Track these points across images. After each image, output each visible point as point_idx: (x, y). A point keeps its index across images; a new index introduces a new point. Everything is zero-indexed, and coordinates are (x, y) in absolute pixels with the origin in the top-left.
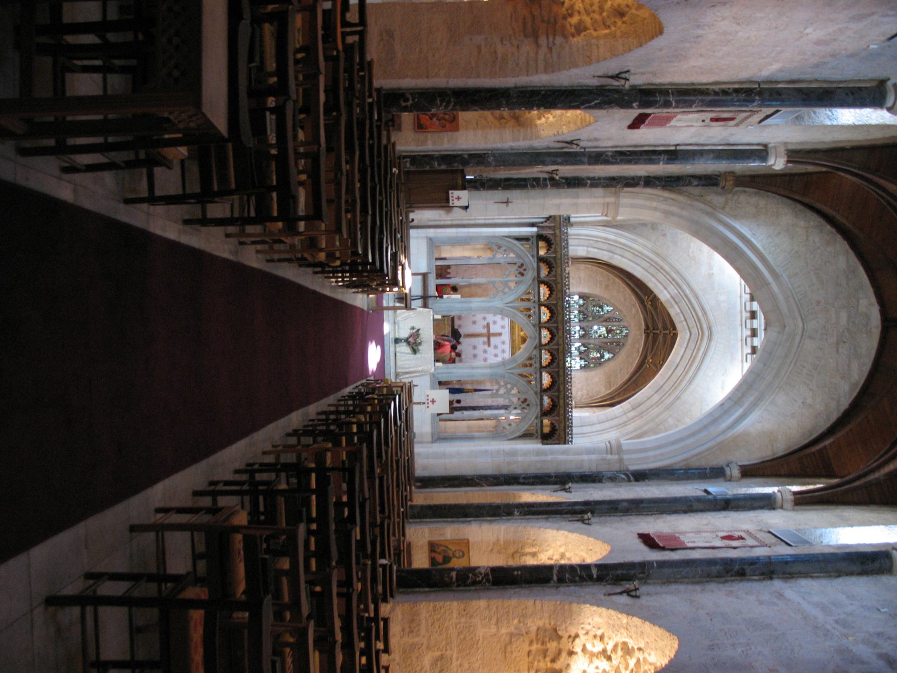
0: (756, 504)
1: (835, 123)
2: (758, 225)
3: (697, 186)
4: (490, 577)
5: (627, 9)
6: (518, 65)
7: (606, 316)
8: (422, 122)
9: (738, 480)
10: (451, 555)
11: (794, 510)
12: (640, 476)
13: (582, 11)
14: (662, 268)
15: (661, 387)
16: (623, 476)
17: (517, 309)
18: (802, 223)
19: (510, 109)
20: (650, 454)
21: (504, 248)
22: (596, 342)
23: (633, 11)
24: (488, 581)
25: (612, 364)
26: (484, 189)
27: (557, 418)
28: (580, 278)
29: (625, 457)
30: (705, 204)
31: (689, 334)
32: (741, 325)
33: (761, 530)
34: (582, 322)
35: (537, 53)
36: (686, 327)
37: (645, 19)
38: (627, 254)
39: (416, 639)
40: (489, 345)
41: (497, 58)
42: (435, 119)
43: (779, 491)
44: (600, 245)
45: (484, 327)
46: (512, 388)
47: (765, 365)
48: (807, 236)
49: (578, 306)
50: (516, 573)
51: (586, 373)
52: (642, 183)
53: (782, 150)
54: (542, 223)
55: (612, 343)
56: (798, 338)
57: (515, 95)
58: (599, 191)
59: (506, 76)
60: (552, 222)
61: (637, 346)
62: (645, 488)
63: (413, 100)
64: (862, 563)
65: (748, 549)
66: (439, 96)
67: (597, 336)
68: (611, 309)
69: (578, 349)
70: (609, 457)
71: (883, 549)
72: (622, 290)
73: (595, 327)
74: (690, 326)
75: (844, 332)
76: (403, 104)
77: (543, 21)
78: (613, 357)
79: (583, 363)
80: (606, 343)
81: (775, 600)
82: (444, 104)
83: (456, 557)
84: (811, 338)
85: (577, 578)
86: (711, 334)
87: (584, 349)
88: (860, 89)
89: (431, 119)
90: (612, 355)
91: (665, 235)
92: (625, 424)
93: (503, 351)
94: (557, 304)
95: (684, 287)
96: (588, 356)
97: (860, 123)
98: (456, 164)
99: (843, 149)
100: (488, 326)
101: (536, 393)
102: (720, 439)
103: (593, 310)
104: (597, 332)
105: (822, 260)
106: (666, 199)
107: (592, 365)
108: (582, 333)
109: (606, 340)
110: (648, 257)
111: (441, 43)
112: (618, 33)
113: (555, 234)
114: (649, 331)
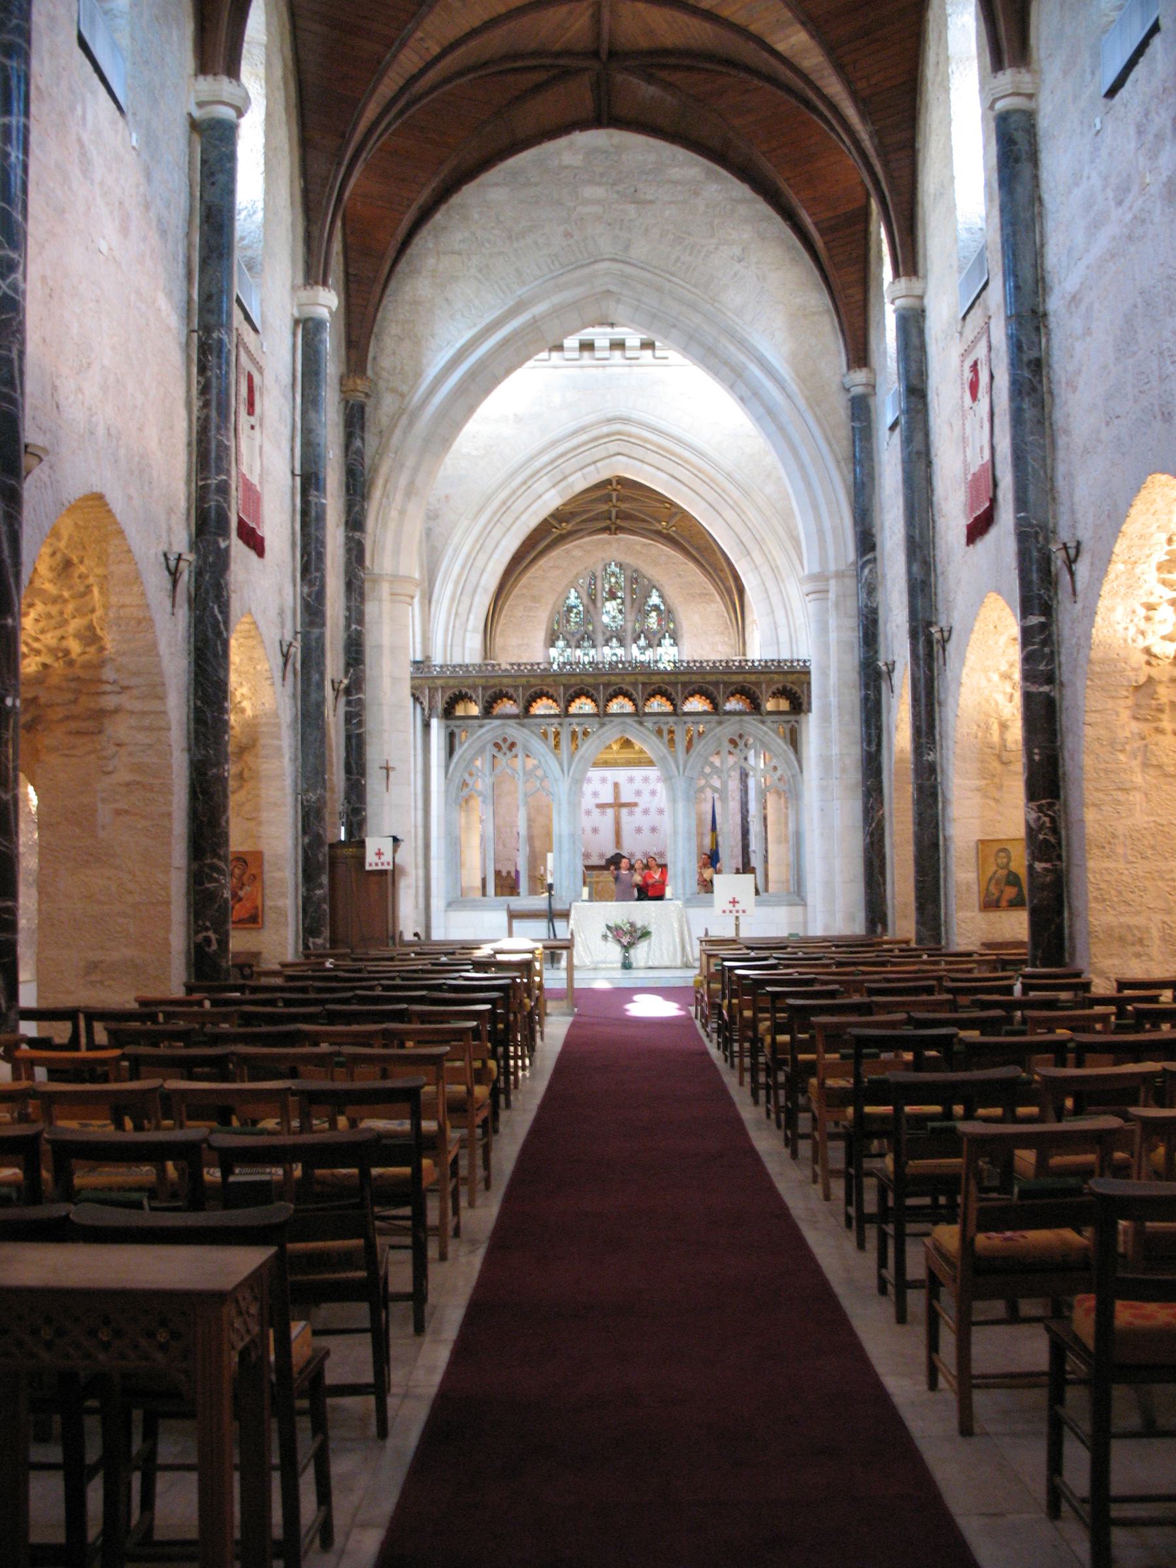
0: (915, 341)
1: (261, 205)
2: (432, 336)
3: (363, 439)
4: (1043, 802)
5: (59, 556)
6: (150, 746)
7: (585, 601)
8: (247, 916)
9: (873, 371)
10: (1005, 872)
11: (925, 277)
12: (866, 542)
13: (59, 633)
14: (504, 503)
15: (710, 505)
16: (866, 571)
17: (572, 756)
18: (431, 261)
19: (227, 761)
20: (827, 524)
21: (466, 776)
22: (631, 617)
23: (62, 544)
24: (1051, 805)
25: (669, 592)
26: (365, 810)
27: (764, 686)
28: (519, 646)
29: (832, 567)
30: (395, 426)
31: (619, 458)
32: (604, 366)
33: (961, 333)
35: (132, 713)
36: (608, 461)
37: (76, 525)
38: (480, 563)
39: (1155, 933)
40: (635, 805)
41: (138, 783)
42: (241, 893)
43: (892, 302)
44: (463, 609)
45: (603, 813)
46: (712, 765)
47: (674, 326)
48: (453, 253)
49: (569, 650)
50: (1037, 758)
51: (686, 636)
52: (357, 535)
53: (304, 295)
54: (423, 709)
55: (633, 591)
56: (628, 270)
57: (203, 752)
58: (370, 608)
59: (170, 766)
60: (422, 693)
61: (638, 548)
62: (887, 533)
63: (207, 929)
64: (1017, 160)
65: (993, 355)
66: (202, 884)
67: (620, 617)
68: (573, 594)
70: (832, 595)
71: (992, 125)
72: (540, 572)
73: (606, 619)
74: (604, 454)
75: (618, 192)
76: (214, 947)
77: (75, 701)
79: (667, 642)
80: (633, 600)
81: (1083, 307)
82: (215, 875)
83: (1008, 863)
84: (627, 247)
85: (1047, 650)
86: (619, 419)
88: (204, 162)
89: (240, 899)
91: (447, 497)
92: (774, 569)
93: (646, 780)
94: (564, 685)
95: (537, 464)
96: (655, 633)
97: (262, 161)
98: (321, 858)
99: (306, 193)
100: (601, 806)
101: (720, 723)
102: (802, 403)
103: (576, 623)
105: (493, 228)
106: (385, 494)
107: (672, 626)
108: (614, 642)
109: (628, 602)
110: (485, 527)
111: (109, 878)
112: (99, 571)
113: (442, 687)
114: (613, 527)
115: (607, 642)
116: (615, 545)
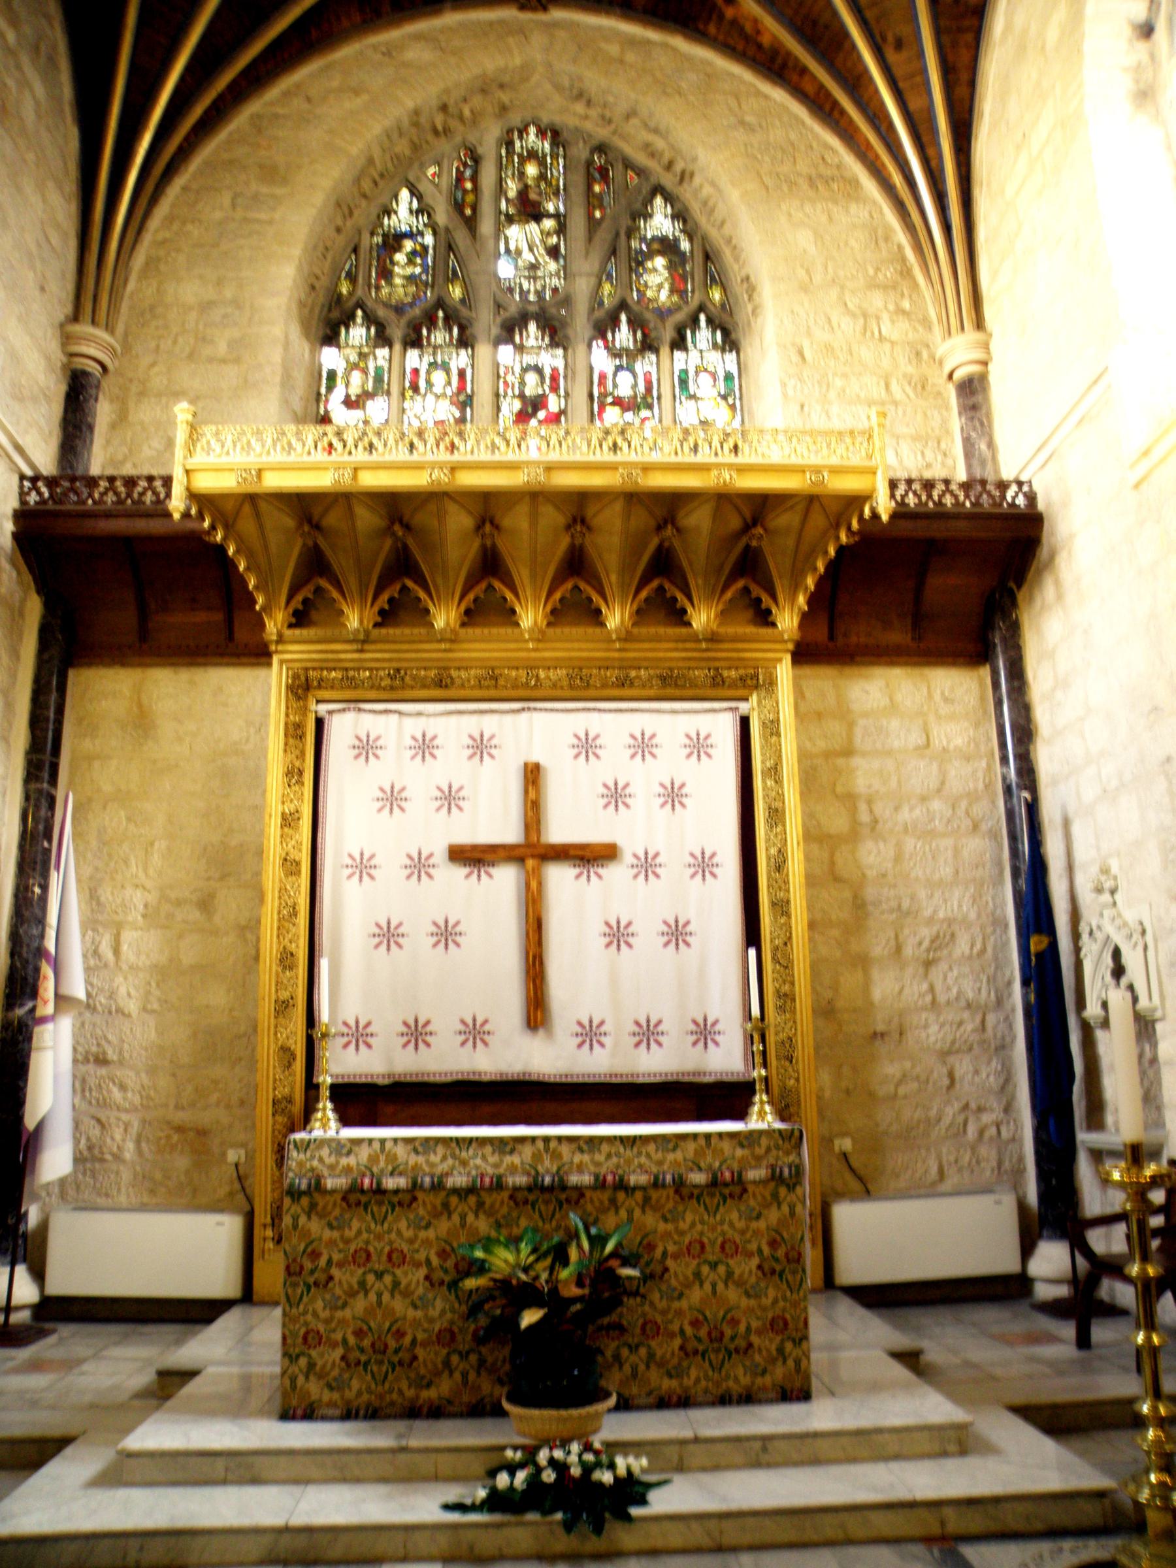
7: (442, 217)
28: (206, 307)
49: (382, 353)
51: (767, 293)
55: (592, 201)
61: (614, 49)
67: (552, 266)
69: (625, 358)
73: (505, 269)
78: (668, 198)
80: (593, 225)
87: (624, 325)
90: (658, 201)
96: (663, 314)
103: (411, 279)
104: (534, 267)
107: (716, 295)
109: (577, 225)
115: (509, 330)
116: (538, 40)
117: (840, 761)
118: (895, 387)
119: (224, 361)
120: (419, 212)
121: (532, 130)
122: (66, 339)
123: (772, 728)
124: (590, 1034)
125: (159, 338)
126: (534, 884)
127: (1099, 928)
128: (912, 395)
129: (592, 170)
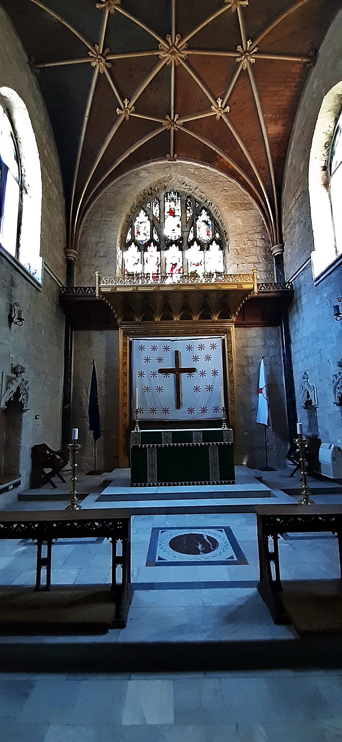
34: (161, 246)
40: (193, 370)
78: (206, 210)
90: (204, 211)
117: (245, 349)
118: (260, 259)
119: (103, 257)
120: (146, 216)
121: (172, 192)
122: (66, 253)
123: (230, 342)
124: (191, 411)
125: (88, 251)
126: (178, 377)
127: (304, 387)
128: (264, 260)
129: (187, 203)
